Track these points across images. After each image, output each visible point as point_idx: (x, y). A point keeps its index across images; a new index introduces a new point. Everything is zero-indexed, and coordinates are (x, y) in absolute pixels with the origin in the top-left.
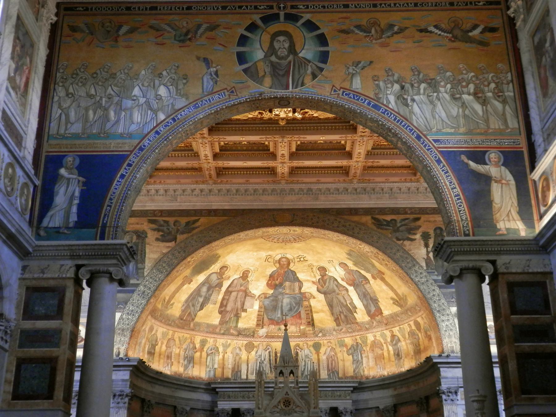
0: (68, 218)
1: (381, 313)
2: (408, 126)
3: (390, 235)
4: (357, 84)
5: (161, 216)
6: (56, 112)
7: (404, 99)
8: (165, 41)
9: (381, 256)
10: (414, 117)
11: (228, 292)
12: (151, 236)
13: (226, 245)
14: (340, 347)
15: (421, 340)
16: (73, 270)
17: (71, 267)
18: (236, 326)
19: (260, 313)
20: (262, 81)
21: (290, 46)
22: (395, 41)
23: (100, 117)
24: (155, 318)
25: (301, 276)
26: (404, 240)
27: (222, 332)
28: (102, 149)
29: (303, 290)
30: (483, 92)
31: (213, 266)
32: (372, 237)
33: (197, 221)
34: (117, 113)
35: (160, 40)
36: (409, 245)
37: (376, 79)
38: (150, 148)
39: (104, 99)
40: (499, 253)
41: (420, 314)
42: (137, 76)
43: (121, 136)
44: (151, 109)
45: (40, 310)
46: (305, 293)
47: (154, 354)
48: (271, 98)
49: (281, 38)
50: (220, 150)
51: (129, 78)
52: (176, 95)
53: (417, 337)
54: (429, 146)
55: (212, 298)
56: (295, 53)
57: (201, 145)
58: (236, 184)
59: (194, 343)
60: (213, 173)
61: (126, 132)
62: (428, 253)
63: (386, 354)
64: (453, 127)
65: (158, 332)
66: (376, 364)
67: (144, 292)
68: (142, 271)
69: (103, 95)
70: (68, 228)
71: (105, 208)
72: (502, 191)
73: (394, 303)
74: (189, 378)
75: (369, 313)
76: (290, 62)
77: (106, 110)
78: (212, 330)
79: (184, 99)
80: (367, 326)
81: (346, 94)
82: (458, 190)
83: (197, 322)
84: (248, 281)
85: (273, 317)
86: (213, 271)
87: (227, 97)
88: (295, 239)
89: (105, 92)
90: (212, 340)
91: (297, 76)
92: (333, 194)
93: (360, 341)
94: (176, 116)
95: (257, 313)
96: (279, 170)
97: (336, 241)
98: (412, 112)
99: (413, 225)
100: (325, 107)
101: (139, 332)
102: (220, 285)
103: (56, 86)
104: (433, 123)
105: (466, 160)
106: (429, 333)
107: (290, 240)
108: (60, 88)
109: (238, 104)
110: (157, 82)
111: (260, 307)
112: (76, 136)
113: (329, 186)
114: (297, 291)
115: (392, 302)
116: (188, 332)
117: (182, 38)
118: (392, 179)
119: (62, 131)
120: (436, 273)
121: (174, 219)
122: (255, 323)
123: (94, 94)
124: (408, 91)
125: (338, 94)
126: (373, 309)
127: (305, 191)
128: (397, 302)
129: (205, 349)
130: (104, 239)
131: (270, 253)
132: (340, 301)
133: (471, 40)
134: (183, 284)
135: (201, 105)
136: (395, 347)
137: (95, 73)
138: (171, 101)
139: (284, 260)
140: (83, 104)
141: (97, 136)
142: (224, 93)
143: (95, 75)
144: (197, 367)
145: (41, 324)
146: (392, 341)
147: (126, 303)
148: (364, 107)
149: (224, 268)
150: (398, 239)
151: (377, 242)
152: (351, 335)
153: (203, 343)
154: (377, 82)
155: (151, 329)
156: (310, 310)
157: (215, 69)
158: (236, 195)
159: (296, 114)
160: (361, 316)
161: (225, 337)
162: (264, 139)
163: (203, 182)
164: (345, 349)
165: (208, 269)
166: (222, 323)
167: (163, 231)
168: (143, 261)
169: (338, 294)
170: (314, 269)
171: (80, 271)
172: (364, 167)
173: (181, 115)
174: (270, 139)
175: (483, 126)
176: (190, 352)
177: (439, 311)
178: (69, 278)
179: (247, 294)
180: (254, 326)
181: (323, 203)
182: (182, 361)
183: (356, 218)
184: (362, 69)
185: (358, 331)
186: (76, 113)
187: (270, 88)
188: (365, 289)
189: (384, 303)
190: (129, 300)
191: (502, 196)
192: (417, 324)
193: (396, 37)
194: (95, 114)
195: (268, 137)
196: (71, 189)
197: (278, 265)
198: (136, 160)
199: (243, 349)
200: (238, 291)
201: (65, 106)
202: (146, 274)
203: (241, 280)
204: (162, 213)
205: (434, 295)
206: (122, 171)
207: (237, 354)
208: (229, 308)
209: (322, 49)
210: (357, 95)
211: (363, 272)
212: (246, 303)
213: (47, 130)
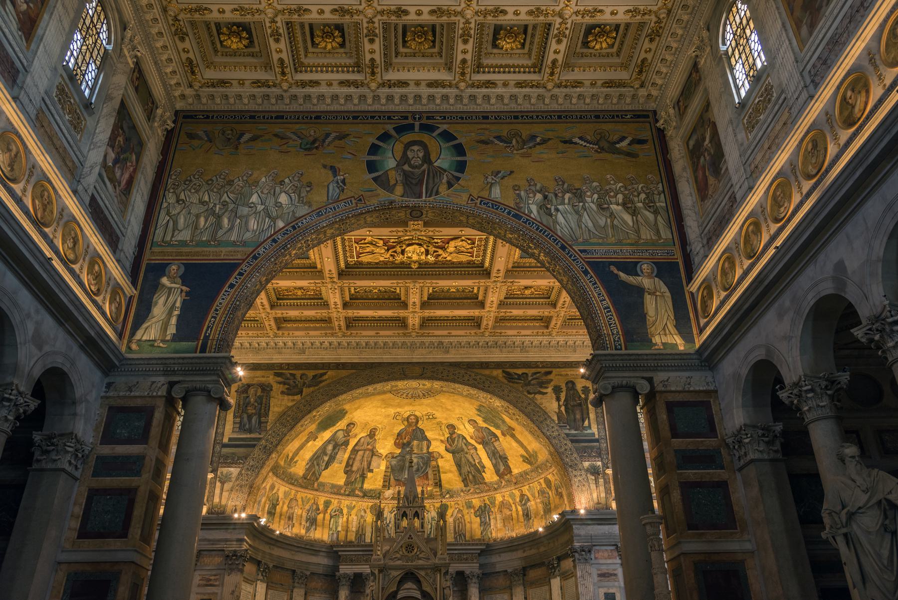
0: (166, 329)
1: (511, 472)
2: (552, 236)
3: (521, 389)
4: (496, 193)
5: (288, 369)
6: (163, 218)
7: (547, 208)
8: (289, 149)
9: (512, 410)
10: (558, 226)
11: (355, 451)
12: (277, 388)
13: (354, 399)
14: (467, 508)
15: (551, 498)
16: (166, 386)
17: (163, 384)
18: (362, 487)
19: (387, 474)
20: (393, 190)
21: (424, 156)
23: (212, 224)
24: (277, 476)
25: (429, 434)
26: (535, 393)
27: (347, 493)
28: (211, 257)
29: (431, 450)
31: (339, 423)
32: (503, 391)
33: (325, 374)
36: (541, 399)
37: (516, 188)
38: (265, 256)
39: (218, 206)
41: (551, 470)
42: (256, 183)
43: (234, 244)
44: (270, 217)
46: (432, 453)
47: (275, 514)
48: (402, 207)
49: (416, 148)
50: (350, 299)
51: (247, 185)
52: (298, 203)
53: (547, 495)
54: (575, 256)
55: (338, 456)
57: (330, 291)
58: (366, 336)
59: (317, 505)
60: (343, 323)
61: (240, 239)
62: (560, 406)
63: (514, 515)
64: (601, 238)
65: (280, 491)
66: (504, 526)
67: (266, 447)
68: (265, 424)
69: (218, 202)
70: (163, 341)
71: (209, 319)
72: (656, 303)
73: (524, 461)
74: (311, 540)
75: (497, 472)
76: (424, 171)
77: (219, 217)
78: (336, 490)
79: (306, 207)
80: (496, 486)
81: (484, 204)
83: (321, 483)
84: (375, 440)
85: (400, 478)
86: (340, 428)
87: (354, 205)
88: (424, 395)
89: (220, 199)
90: (336, 501)
91: (431, 185)
92: (464, 347)
93: (488, 502)
94: (297, 224)
95: (383, 474)
96: (410, 322)
97: (466, 396)
98: (556, 222)
99: (544, 378)
100: (461, 218)
101: (259, 489)
102: (346, 443)
103: (167, 192)
104: (578, 233)
105: (616, 271)
106: (560, 490)
107: (419, 396)
108: (170, 194)
109: (366, 213)
110: (278, 189)
111: (387, 468)
112: (183, 243)
113: (460, 339)
114: (425, 451)
115: (522, 459)
116: (311, 492)
117: (308, 146)
118: (524, 332)
119: (168, 238)
120: (568, 427)
121: (301, 372)
122: (381, 483)
123: (208, 200)
124: (551, 201)
125: (476, 203)
126: (502, 468)
127: (436, 344)
128: (527, 459)
129: (329, 511)
130: (205, 352)
131: (399, 410)
132: (468, 461)
134: (307, 441)
135: (325, 213)
136: (524, 507)
137: (211, 180)
138: (292, 209)
139: (412, 417)
140: (194, 211)
142: (351, 201)
143: (210, 182)
144: (319, 529)
145: (122, 450)
146: (521, 501)
147: (246, 459)
148: (504, 216)
149: (351, 424)
150: (529, 393)
151: (508, 396)
152: (479, 496)
153: (327, 504)
154: (518, 192)
155: (272, 487)
156: (437, 470)
157: (342, 177)
158: (366, 348)
159: (429, 256)
160: (490, 475)
161: (350, 498)
162: (396, 285)
163: (332, 335)
164: (472, 511)
165: (334, 425)
166: (347, 483)
167: (289, 384)
168: (267, 415)
169: (467, 453)
170: (443, 427)
171: (173, 389)
172: (496, 318)
173: (302, 223)
174: (401, 285)
175: (633, 236)
176: (313, 514)
177: (571, 466)
178: (160, 397)
179: (373, 453)
180: (380, 487)
181: (453, 356)
182: (303, 523)
183: (487, 372)
184: (502, 179)
185: (486, 492)
186: (185, 220)
187: (402, 196)
188: (494, 446)
189: (514, 462)
190: (250, 455)
191: (657, 309)
192: (548, 482)
194: (206, 221)
195: (399, 281)
196: (171, 299)
197: (406, 423)
198: (248, 270)
199: (368, 511)
200: (365, 450)
202: (268, 428)
203: (368, 439)
204: (289, 366)
205: (566, 450)
206: (232, 280)
207: (362, 517)
208: (355, 468)
209: (459, 159)
210: (496, 205)
211: (493, 429)
212: (372, 463)
213: (151, 238)
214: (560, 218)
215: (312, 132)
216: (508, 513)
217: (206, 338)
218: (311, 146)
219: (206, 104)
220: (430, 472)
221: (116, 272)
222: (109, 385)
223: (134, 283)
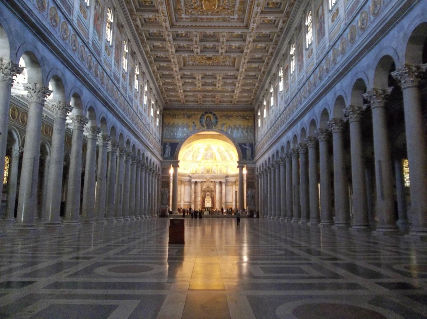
6: (164, 133)
11: (194, 152)
22: (231, 119)
34: (176, 134)
43: (178, 139)
49: (208, 118)
77: (174, 133)
98: (233, 135)
102: (192, 151)
112: (169, 139)
156: (215, 157)
160: (228, 158)
179: (199, 152)
209: (217, 120)
214: (234, 134)
215: (190, 113)
218: (189, 117)
222: (162, 165)
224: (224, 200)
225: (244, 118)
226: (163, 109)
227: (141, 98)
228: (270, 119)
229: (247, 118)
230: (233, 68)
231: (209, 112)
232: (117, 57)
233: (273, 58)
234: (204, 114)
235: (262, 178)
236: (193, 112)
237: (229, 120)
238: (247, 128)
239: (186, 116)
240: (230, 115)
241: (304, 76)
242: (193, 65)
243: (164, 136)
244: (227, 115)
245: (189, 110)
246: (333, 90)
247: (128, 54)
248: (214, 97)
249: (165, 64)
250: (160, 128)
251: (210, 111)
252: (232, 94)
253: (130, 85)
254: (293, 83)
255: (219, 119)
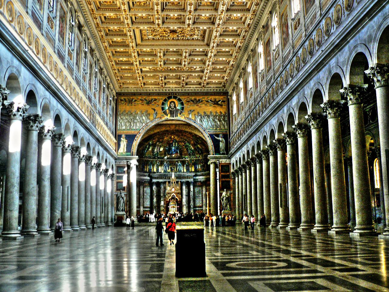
4: (190, 116)
6: (119, 123)
22: (199, 104)
30: (220, 119)
35: (143, 103)
40: (220, 159)
43: (135, 130)
45: (120, 171)
49: (172, 103)
56: (176, 108)
70: (124, 152)
77: (131, 123)
82: (212, 144)
98: (203, 124)
104: (208, 127)
112: (124, 130)
133: (218, 104)
140: (125, 121)
141: (129, 130)
193: (201, 103)
201: (121, 122)
206: (136, 139)
208: (155, 151)
209: (182, 106)
210: (190, 119)
216: (202, 164)
217: (132, 152)
218: (149, 103)
219: (123, 91)
220: (178, 152)
221: (114, 139)
222: (115, 162)
223: (116, 139)
224: (192, 203)
225: (216, 103)
226: (117, 93)
227: (90, 80)
228: (248, 104)
229: (220, 103)
230: (202, 43)
231: (172, 98)
232: (61, 31)
233: (251, 30)
234: (167, 99)
235: (240, 177)
236: (153, 97)
237: (197, 105)
238: (220, 116)
239: (146, 102)
240: (199, 100)
241: (290, 51)
242: (153, 39)
243: (118, 127)
244: (195, 99)
245: (149, 94)
246: (327, 66)
247: (75, 28)
248: (180, 78)
249: (119, 39)
250: (113, 117)
251: (174, 95)
252: (201, 74)
253: (77, 64)
254: (277, 60)
255: (185, 105)
